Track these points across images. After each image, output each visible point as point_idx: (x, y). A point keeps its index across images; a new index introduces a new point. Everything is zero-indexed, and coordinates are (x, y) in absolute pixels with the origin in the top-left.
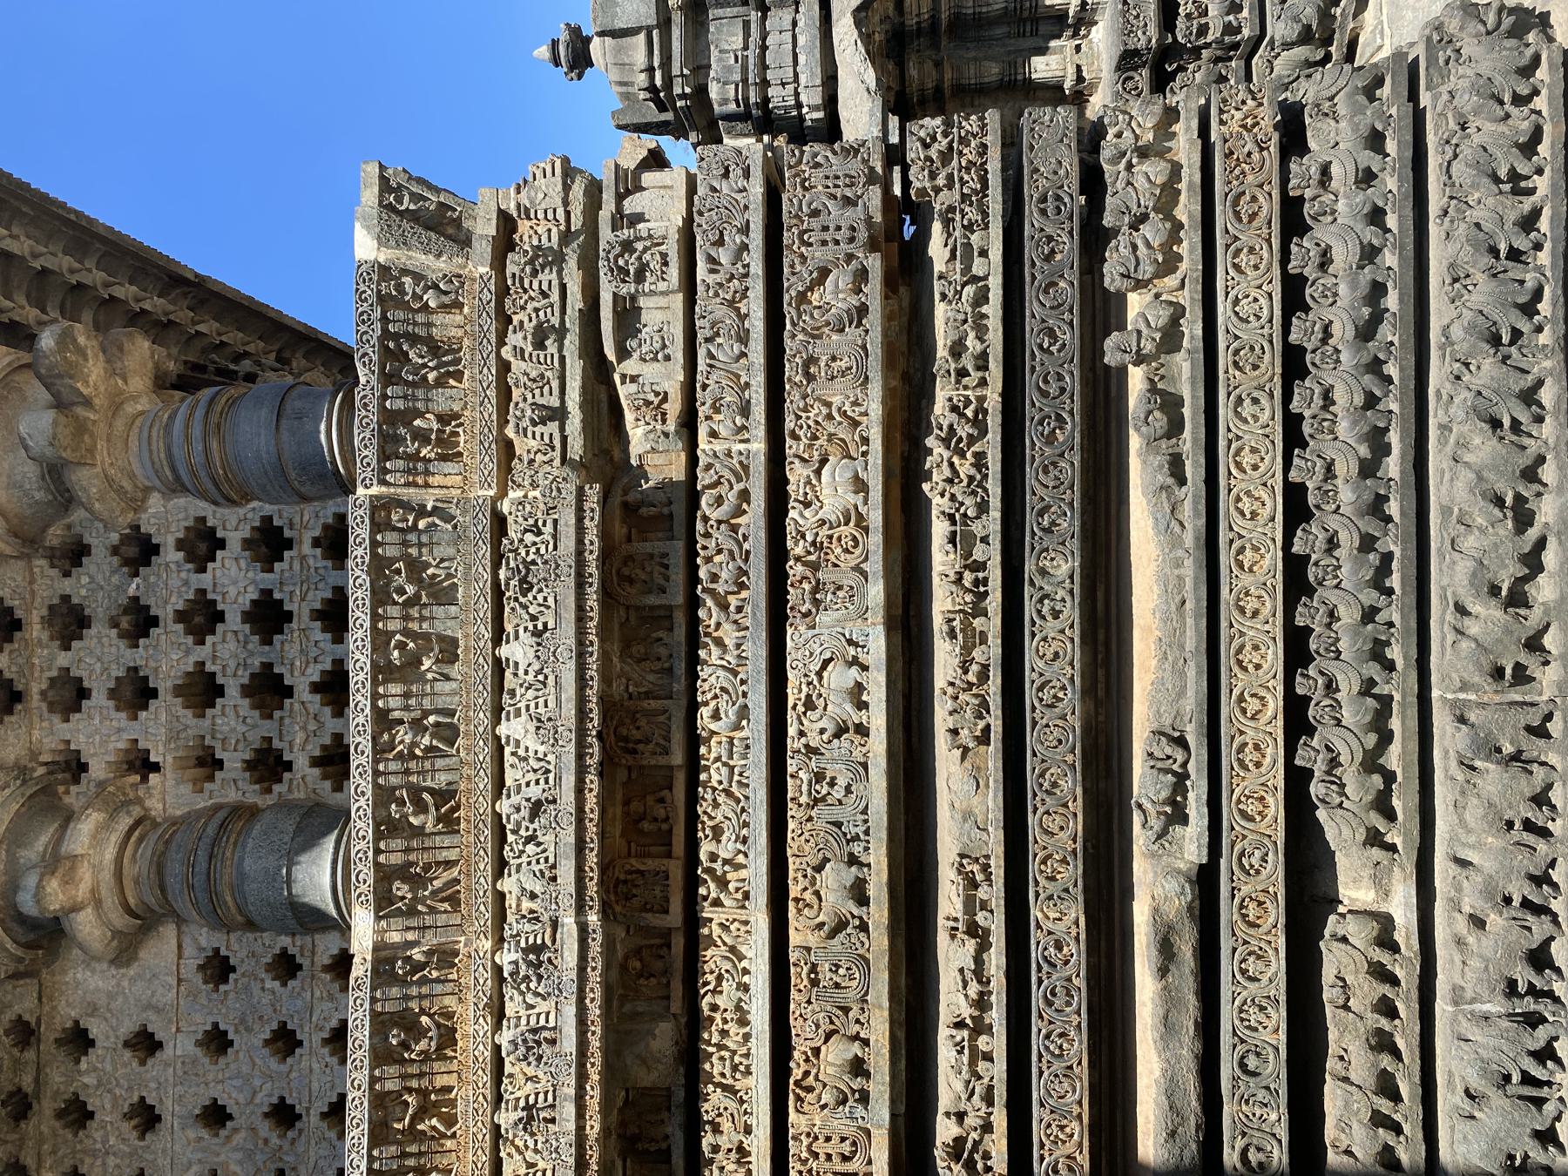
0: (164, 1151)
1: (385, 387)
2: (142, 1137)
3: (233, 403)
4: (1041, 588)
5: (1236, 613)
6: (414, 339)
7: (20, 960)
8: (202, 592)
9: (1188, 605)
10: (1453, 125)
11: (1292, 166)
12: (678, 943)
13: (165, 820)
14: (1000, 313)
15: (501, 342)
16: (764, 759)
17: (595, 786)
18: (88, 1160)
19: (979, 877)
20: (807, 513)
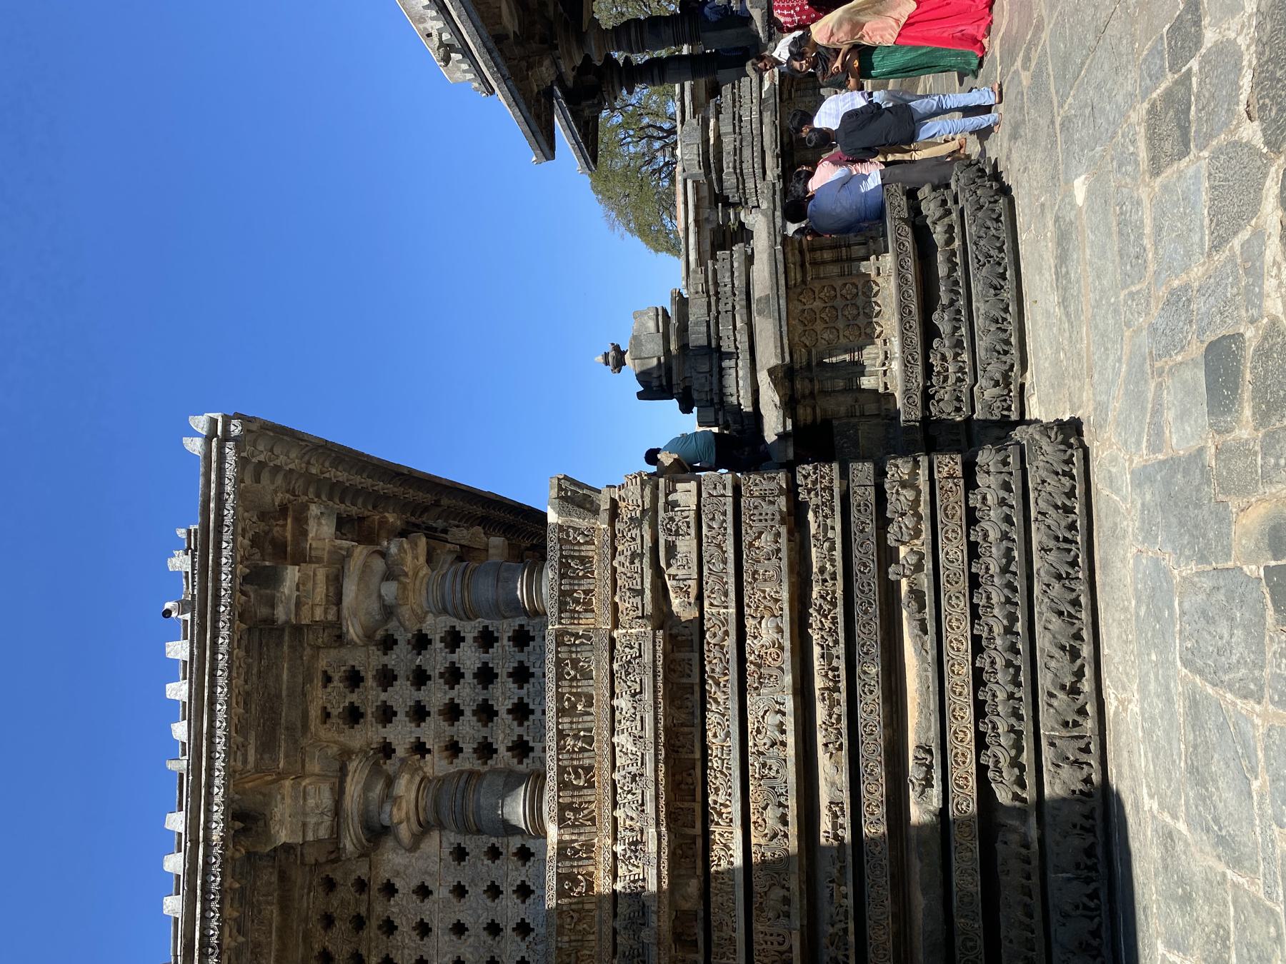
0: (433, 947)
2: (422, 939)
3: (473, 571)
6: (573, 558)
7: (363, 847)
8: (453, 663)
9: (931, 689)
10: (1039, 481)
12: (699, 842)
13: (434, 778)
15: (613, 557)
17: (663, 769)
18: (394, 952)
19: (839, 813)
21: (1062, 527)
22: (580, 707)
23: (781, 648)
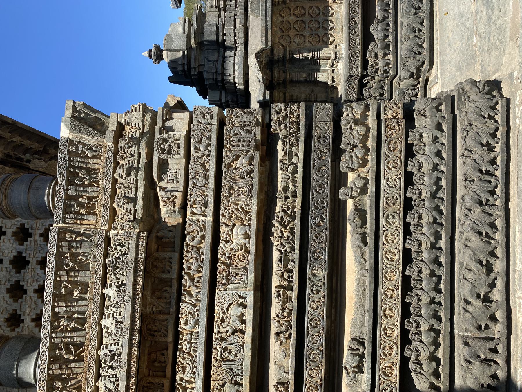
1: (68, 186)
4: (313, 281)
5: (384, 296)
6: (81, 168)
9: (367, 291)
10: (466, 123)
11: (410, 133)
14: (302, 177)
15: (114, 171)
16: (204, 342)
17: (136, 352)
20: (226, 245)
21: (486, 162)
22: (76, 294)
23: (248, 251)
